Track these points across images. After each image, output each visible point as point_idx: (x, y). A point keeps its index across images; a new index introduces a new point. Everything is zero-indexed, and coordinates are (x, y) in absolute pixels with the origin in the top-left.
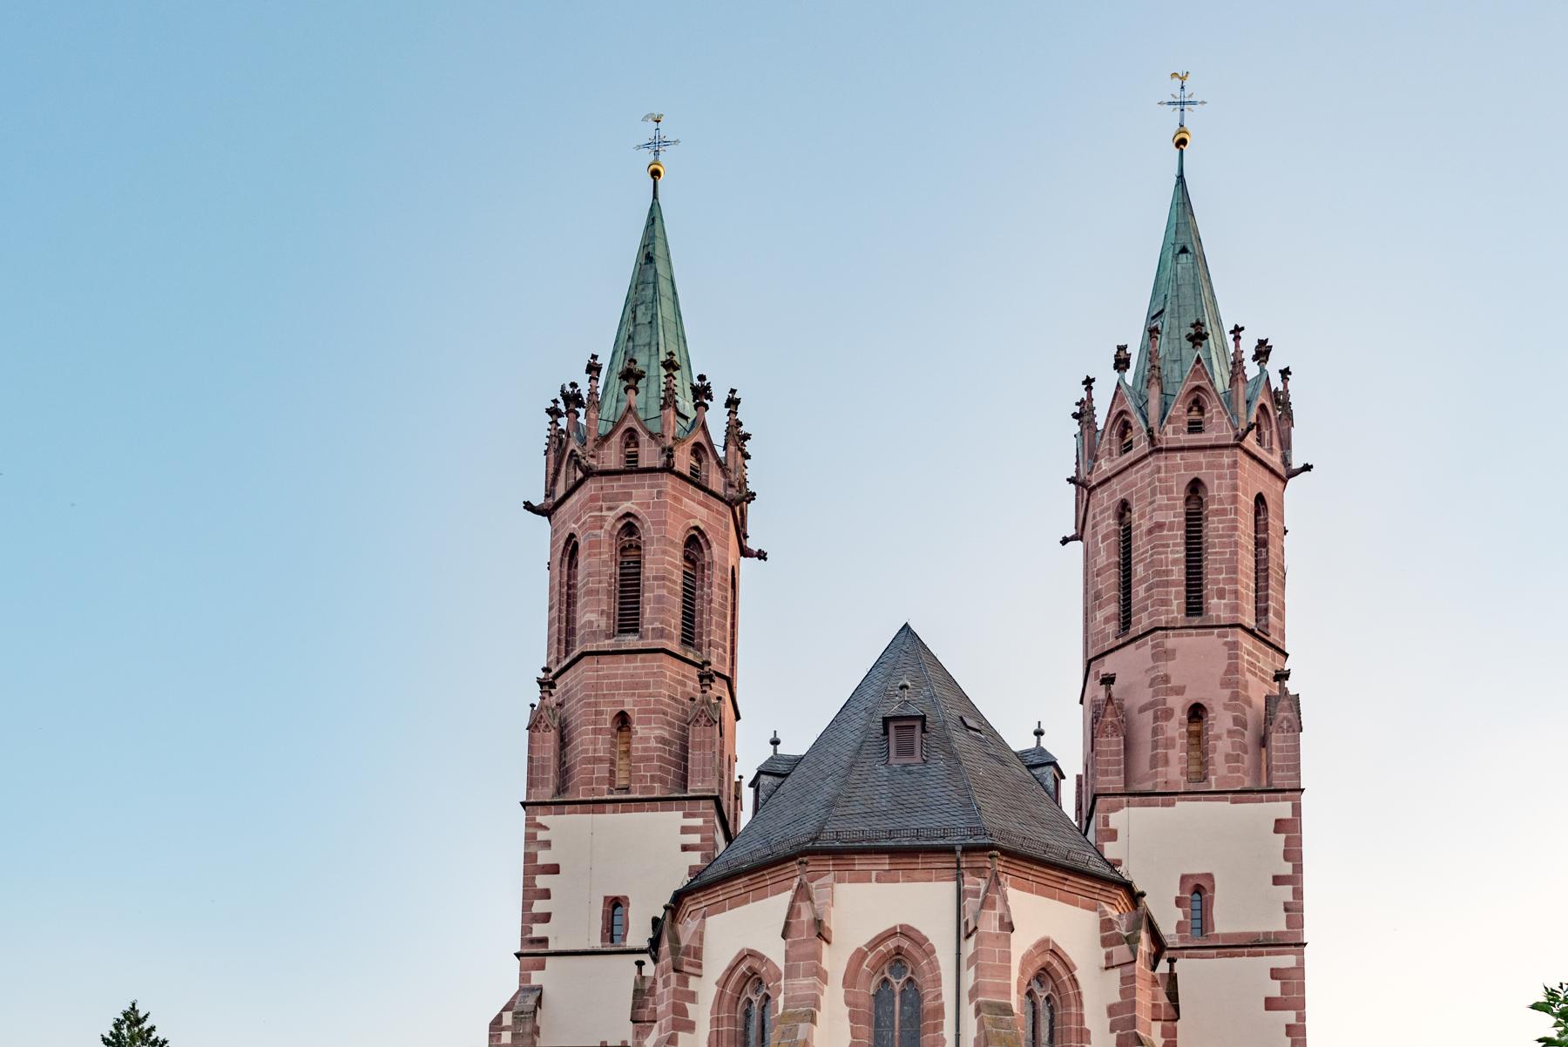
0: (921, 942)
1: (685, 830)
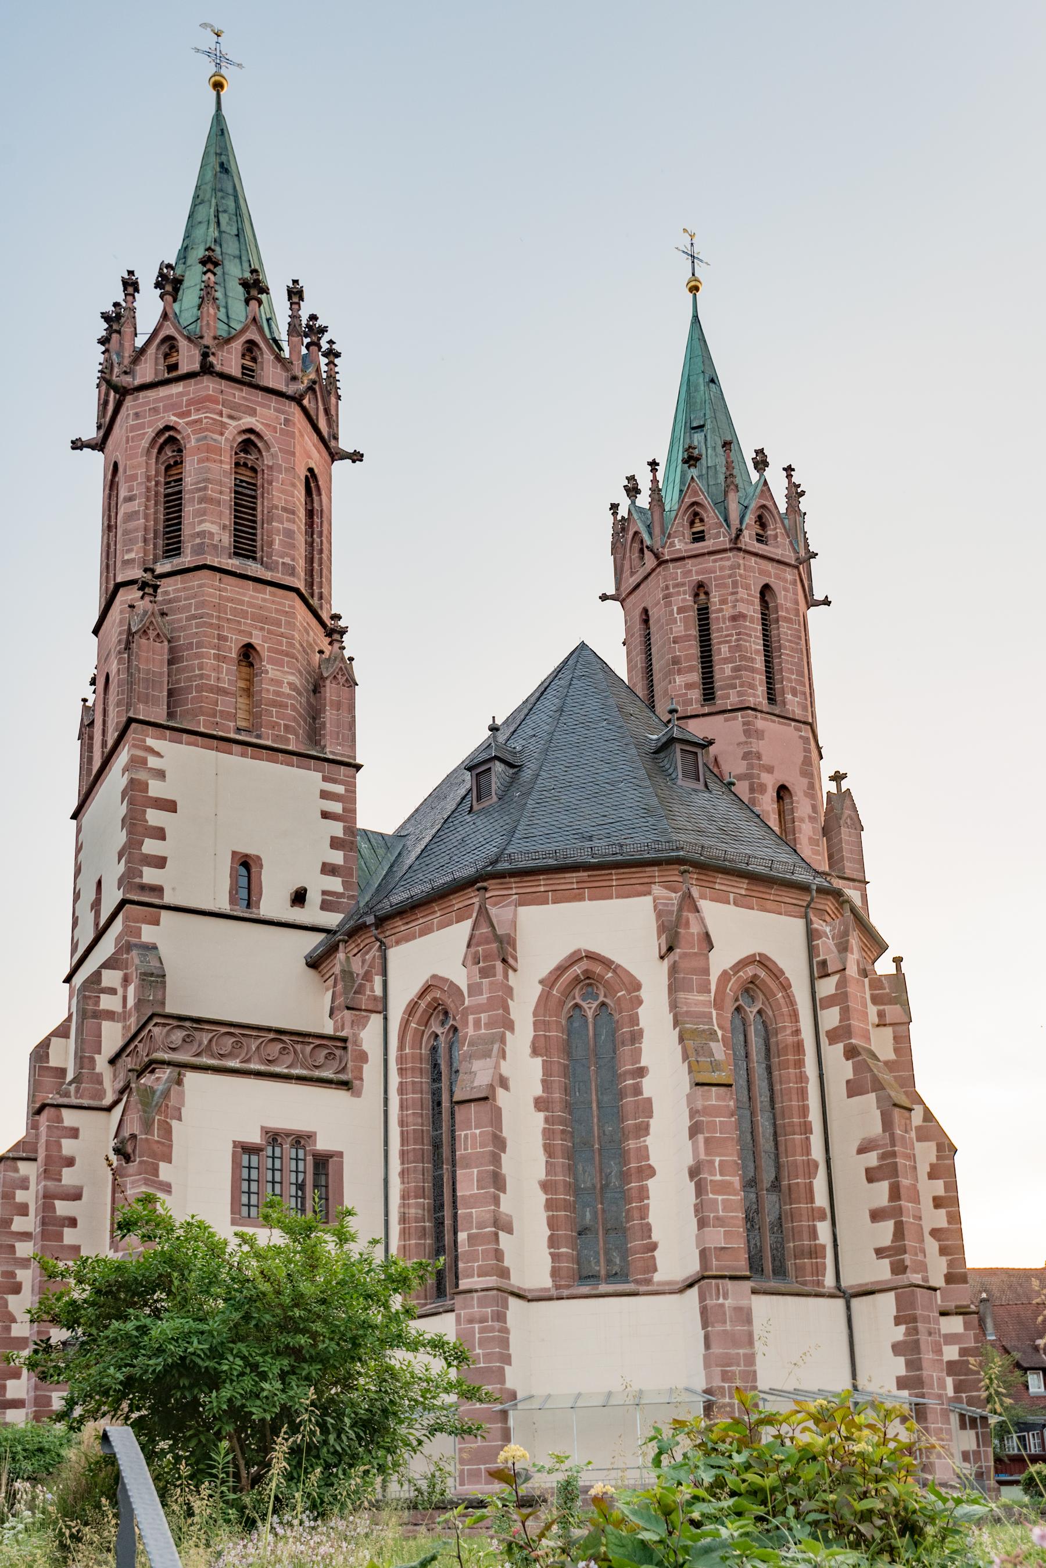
0: (778, 974)
1: (325, 795)
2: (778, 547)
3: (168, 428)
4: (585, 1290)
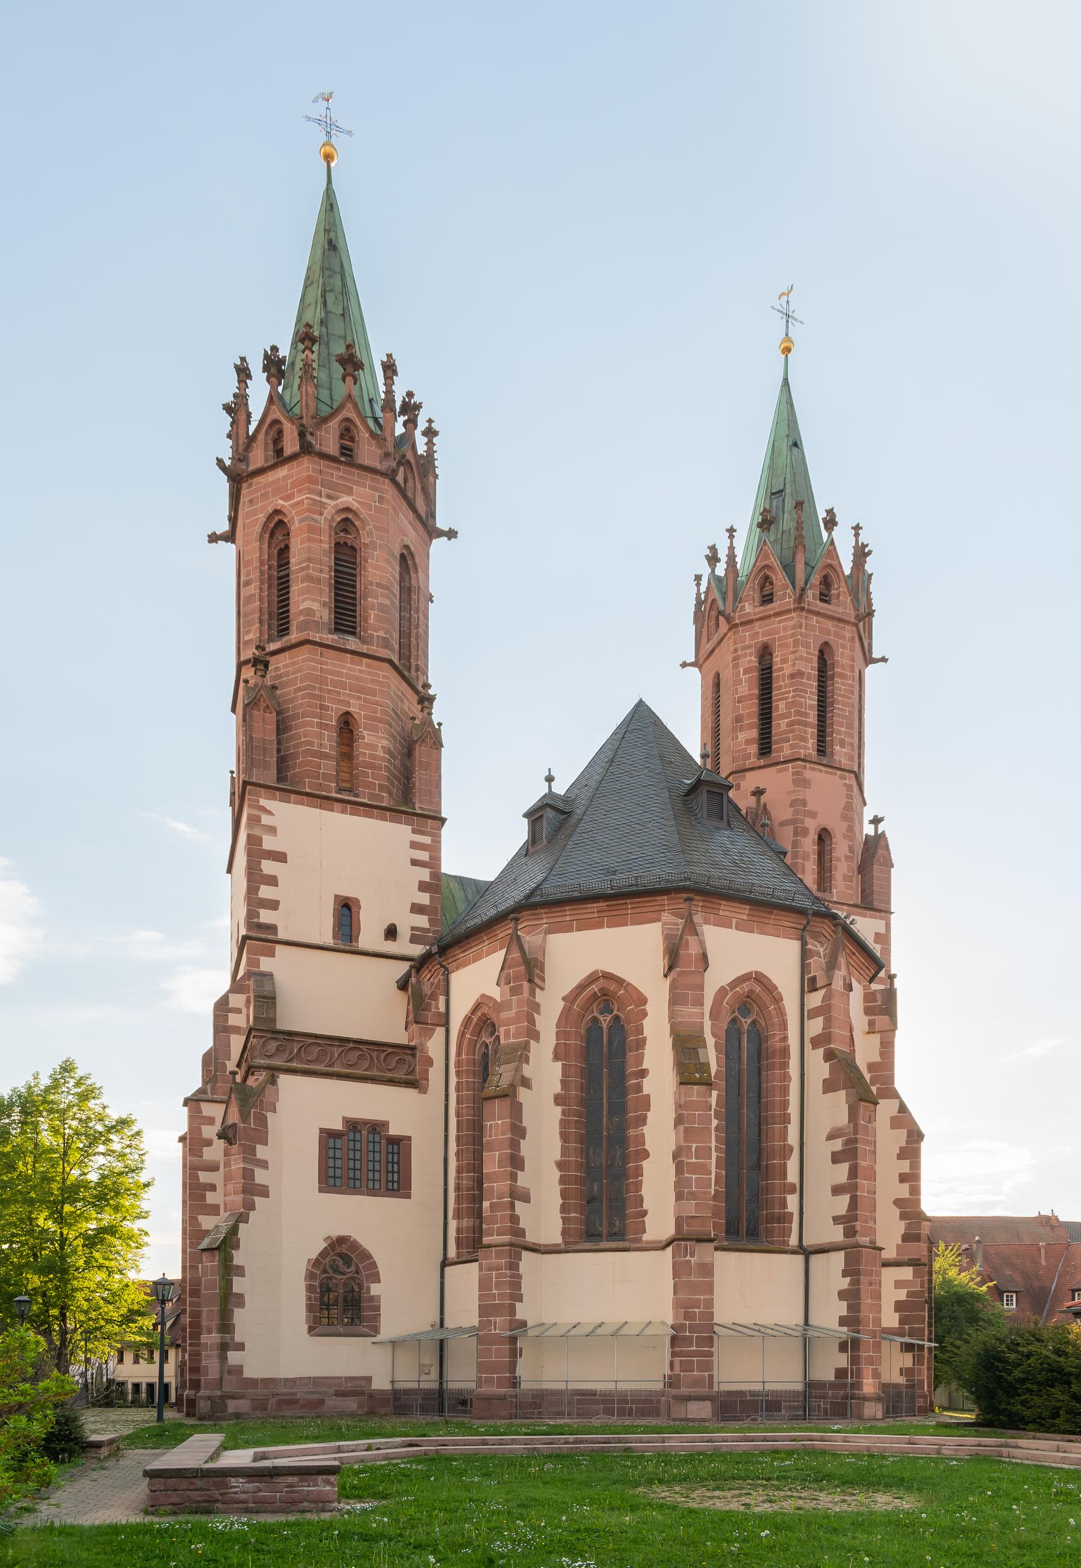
2: (839, 606)
3: (277, 512)
4: (588, 1246)
